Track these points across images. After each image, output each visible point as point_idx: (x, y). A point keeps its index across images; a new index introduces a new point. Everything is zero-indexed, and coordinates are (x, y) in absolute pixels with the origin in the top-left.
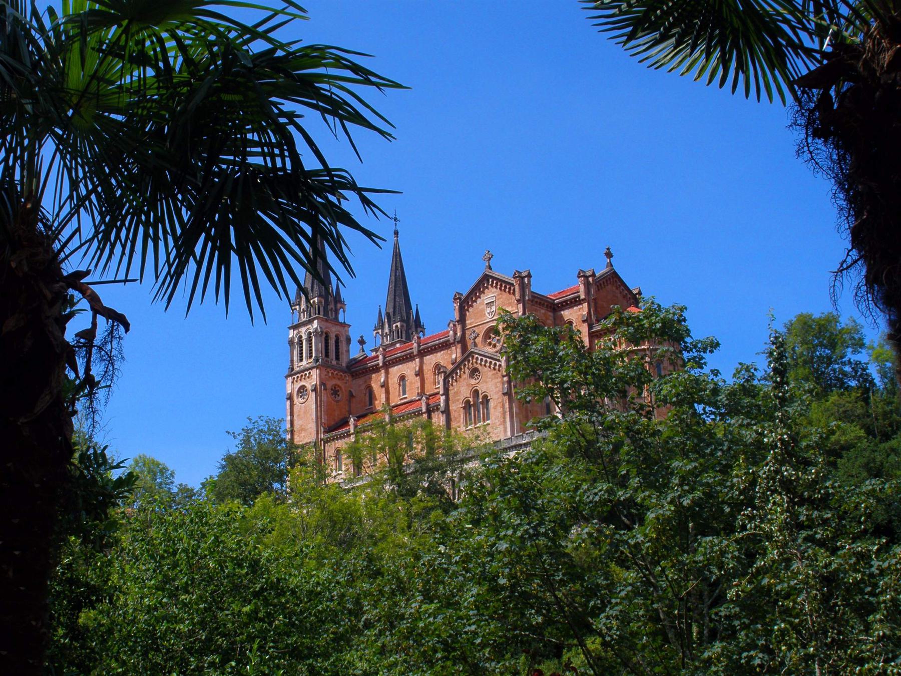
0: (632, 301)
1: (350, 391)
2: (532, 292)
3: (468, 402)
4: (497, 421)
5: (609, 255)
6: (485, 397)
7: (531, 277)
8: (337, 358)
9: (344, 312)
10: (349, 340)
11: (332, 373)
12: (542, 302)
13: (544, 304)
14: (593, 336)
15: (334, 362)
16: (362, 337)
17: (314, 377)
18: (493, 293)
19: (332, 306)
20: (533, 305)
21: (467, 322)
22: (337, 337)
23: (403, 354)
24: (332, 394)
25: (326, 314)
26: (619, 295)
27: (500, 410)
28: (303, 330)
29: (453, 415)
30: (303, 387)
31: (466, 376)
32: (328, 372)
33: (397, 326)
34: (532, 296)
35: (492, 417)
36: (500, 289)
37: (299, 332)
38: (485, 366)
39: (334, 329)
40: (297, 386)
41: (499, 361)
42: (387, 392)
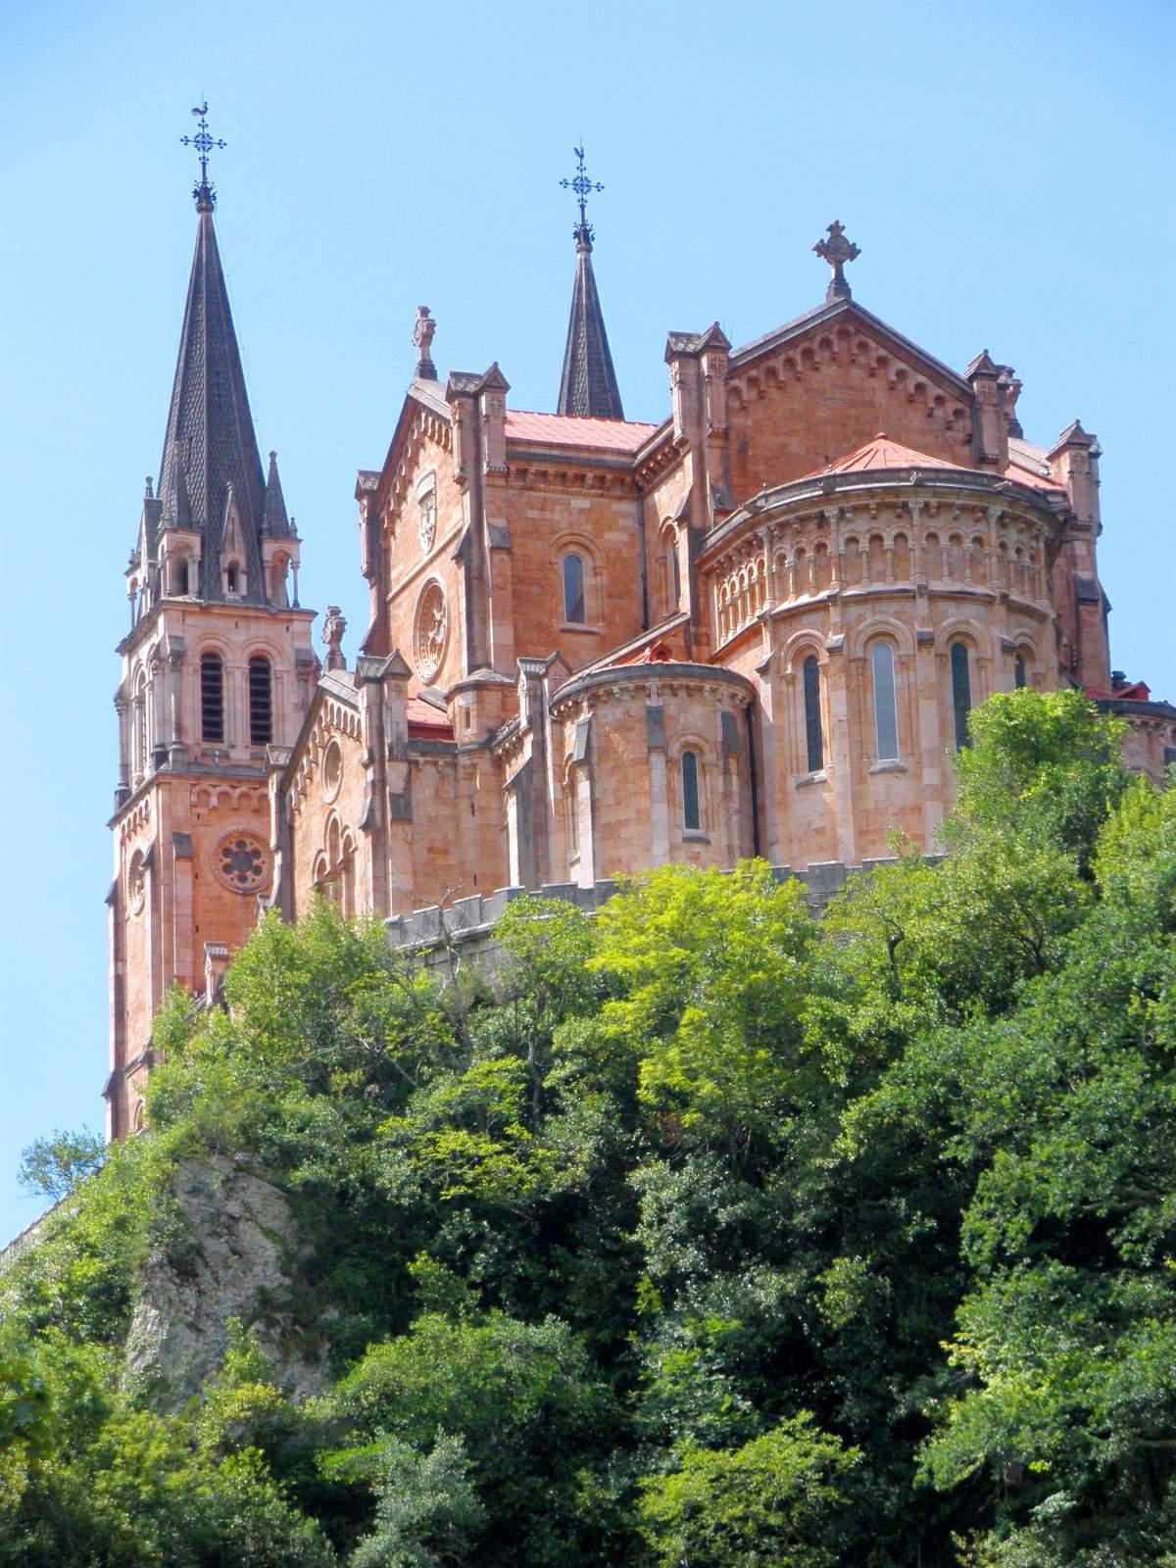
2: (512, 442)
5: (837, 248)
7: (504, 387)
8: (261, 731)
11: (224, 795)
12: (571, 472)
13: (581, 478)
15: (241, 754)
19: (235, 554)
20: (532, 489)
21: (394, 574)
24: (227, 869)
25: (209, 587)
26: (881, 397)
31: (318, 775)
34: (511, 457)
37: (139, 665)
39: (240, 637)
41: (355, 707)
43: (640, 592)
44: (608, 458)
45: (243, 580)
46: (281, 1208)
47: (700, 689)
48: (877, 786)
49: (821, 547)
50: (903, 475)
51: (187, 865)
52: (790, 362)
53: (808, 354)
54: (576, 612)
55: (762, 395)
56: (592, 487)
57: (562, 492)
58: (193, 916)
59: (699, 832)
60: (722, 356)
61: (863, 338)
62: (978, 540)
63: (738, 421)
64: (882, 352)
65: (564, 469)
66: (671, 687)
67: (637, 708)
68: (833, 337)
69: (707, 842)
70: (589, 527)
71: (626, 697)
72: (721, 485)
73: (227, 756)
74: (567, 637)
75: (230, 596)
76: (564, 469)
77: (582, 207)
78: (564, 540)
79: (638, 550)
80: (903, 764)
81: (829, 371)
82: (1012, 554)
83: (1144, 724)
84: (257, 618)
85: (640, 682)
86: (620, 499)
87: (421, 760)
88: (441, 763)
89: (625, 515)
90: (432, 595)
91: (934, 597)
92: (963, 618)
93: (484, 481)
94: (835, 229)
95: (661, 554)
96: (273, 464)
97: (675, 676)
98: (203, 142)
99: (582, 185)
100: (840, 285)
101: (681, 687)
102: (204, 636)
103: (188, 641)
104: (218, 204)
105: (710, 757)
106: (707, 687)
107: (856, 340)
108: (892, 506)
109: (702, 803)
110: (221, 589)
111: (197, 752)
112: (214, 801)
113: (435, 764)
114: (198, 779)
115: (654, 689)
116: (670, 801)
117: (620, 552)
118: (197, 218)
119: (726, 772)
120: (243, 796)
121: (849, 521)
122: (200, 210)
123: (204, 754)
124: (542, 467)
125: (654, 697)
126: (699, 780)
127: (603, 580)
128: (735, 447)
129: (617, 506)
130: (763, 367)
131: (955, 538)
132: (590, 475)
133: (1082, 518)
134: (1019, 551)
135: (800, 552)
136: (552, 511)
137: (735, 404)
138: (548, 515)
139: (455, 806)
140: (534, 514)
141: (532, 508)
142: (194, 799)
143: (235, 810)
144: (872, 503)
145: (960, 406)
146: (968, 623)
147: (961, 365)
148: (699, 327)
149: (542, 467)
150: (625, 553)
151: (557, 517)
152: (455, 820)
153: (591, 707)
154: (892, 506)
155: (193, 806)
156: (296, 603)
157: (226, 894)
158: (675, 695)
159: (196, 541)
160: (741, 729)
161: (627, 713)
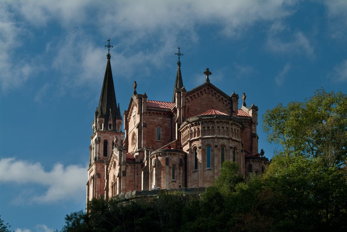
13: (161, 114)
19: (111, 122)
20: (152, 116)
21: (129, 130)
26: (215, 100)
34: (147, 110)
43: (171, 134)
44: (166, 110)
45: (112, 127)
47: (176, 154)
50: (214, 116)
51: (99, 179)
52: (198, 94)
53: (201, 92)
56: (162, 115)
57: (157, 116)
58: (100, 188)
59: (174, 180)
60: (185, 93)
61: (212, 89)
62: (227, 128)
63: (187, 104)
64: (215, 92)
65: (157, 112)
66: (170, 153)
68: (206, 89)
69: (176, 182)
70: (162, 123)
72: (184, 116)
74: (157, 143)
75: (109, 130)
76: (157, 112)
77: (179, 58)
78: (157, 125)
79: (171, 127)
80: (211, 169)
81: (205, 95)
82: (234, 130)
83: (258, 161)
84: (114, 134)
85: (165, 153)
86: (168, 117)
87: (128, 165)
88: (132, 165)
90: (134, 134)
91: (218, 138)
92: (223, 142)
94: (208, 69)
96: (119, 106)
100: (208, 80)
101: (172, 154)
104: (111, 58)
105: (177, 166)
106: (177, 154)
107: (210, 90)
108: (211, 121)
110: (108, 129)
111: (102, 158)
113: (131, 166)
114: (102, 163)
115: (167, 154)
116: (170, 175)
117: (167, 127)
118: (107, 60)
119: (180, 169)
121: (204, 124)
122: (108, 59)
123: (103, 159)
124: (153, 112)
125: (167, 155)
126: (175, 170)
127: (164, 132)
128: (186, 110)
129: (167, 119)
130: (193, 94)
131: (223, 127)
132: (162, 113)
133: (254, 122)
134: (235, 130)
136: (155, 120)
137: (187, 101)
139: (134, 173)
140: (152, 120)
141: (151, 119)
142: (101, 167)
144: (208, 121)
145: (229, 102)
146: (224, 143)
147: (230, 95)
149: (153, 112)
150: (168, 127)
151: (156, 121)
152: (134, 176)
154: (211, 121)
155: (101, 168)
158: (171, 155)
159: (104, 120)
160: (183, 161)
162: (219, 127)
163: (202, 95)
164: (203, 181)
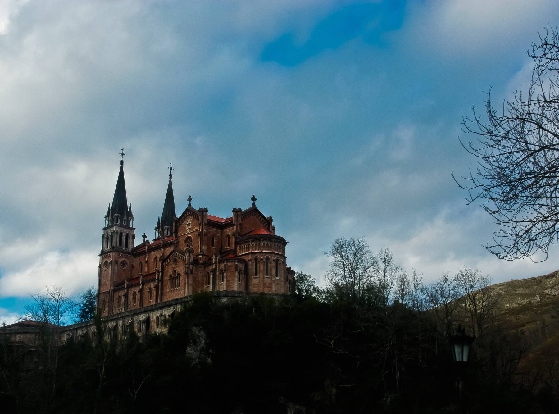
0: (266, 223)
1: (132, 264)
2: (208, 219)
3: (171, 276)
4: (182, 288)
5: (254, 199)
6: (179, 274)
8: (127, 245)
9: (133, 221)
10: (134, 237)
11: (122, 255)
14: (236, 243)
15: (124, 249)
16: (145, 234)
17: (112, 256)
18: (191, 219)
19: (125, 218)
20: (208, 226)
21: (179, 233)
22: (127, 235)
23: (156, 246)
24: (121, 266)
26: (258, 221)
27: (184, 282)
28: (109, 230)
29: (165, 282)
30: (106, 261)
32: (119, 254)
33: (165, 228)
34: (208, 222)
35: (181, 285)
36: (193, 217)
38: (180, 258)
39: (125, 231)
40: (104, 261)
42: (148, 266)
46: (205, 335)
47: (242, 262)
48: (266, 280)
49: (259, 244)
53: (250, 214)
54: (213, 245)
55: (244, 219)
59: (240, 282)
62: (280, 246)
64: (259, 215)
67: (233, 263)
69: (241, 284)
71: (232, 262)
73: (122, 249)
74: (212, 249)
77: (171, 172)
81: (252, 216)
89: (220, 232)
93: (204, 225)
95: (226, 238)
97: (239, 260)
98: (122, 154)
99: (171, 168)
100: (254, 204)
102: (120, 230)
103: (119, 230)
109: (241, 278)
112: (121, 255)
120: (125, 255)
131: (277, 246)
135: (256, 244)
138: (211, 230)
140: (209, 230)
143: (123, 257)
144: (268, 239)
148: (237, 208)
153: (226, 262)
156: (132, 227)
157: (121, 270)
161: (232, 264)
162: (275, 245)
163: (251, 215)
164: (263, 286)
